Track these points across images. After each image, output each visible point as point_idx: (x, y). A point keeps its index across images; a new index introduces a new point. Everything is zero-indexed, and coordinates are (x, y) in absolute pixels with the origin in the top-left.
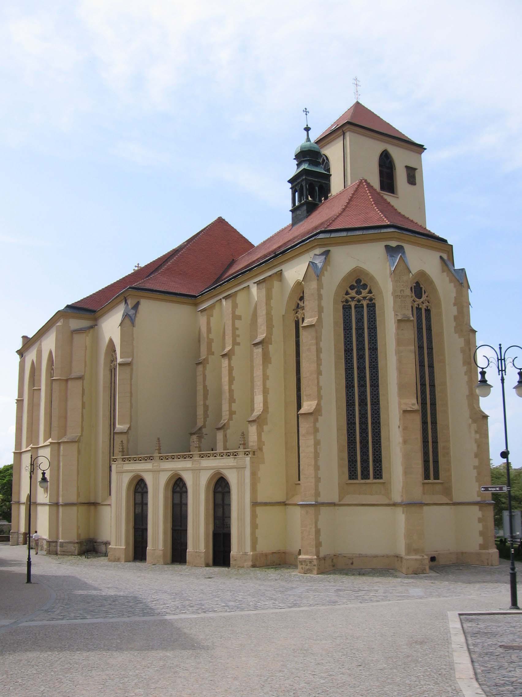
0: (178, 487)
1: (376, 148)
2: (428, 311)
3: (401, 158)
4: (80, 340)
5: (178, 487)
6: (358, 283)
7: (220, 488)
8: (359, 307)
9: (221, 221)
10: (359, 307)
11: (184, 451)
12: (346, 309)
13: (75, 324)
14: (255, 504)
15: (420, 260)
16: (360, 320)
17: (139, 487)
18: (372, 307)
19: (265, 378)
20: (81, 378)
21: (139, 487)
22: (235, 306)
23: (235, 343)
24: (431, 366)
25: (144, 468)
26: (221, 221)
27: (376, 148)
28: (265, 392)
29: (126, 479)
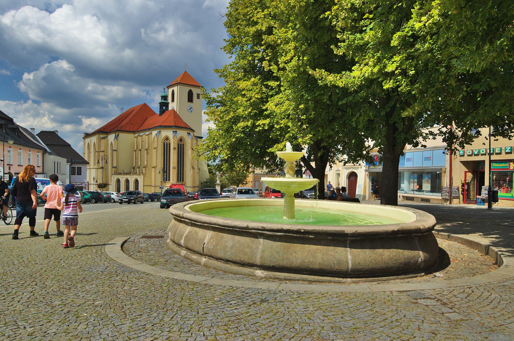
0: (127, 181)
1: (188, 89)
2: (183, 145)
3: (195, 91)
4: (103, 141)
5: (127, 181)
6: (167, 138)
7: (137, 182)
8: (167, 144)
9: (145, 104)
10: (167, 144)
11: (129, 174)
12: (164, 144)
13: (102, 136)
14: (144, 186)
15: (182, 133)
16: (167, 147)
17: (118, 181)
18: (170, 144)
19: (147, 158)
20: (104, 151)
21: (118, 181)
22: (142, 139)
23: (142, 148)
24: (183, 157)
25: (120, 177)
26: (145, 104)
27: (188, 89)
28: (147, 161)
29: (115, 179)
